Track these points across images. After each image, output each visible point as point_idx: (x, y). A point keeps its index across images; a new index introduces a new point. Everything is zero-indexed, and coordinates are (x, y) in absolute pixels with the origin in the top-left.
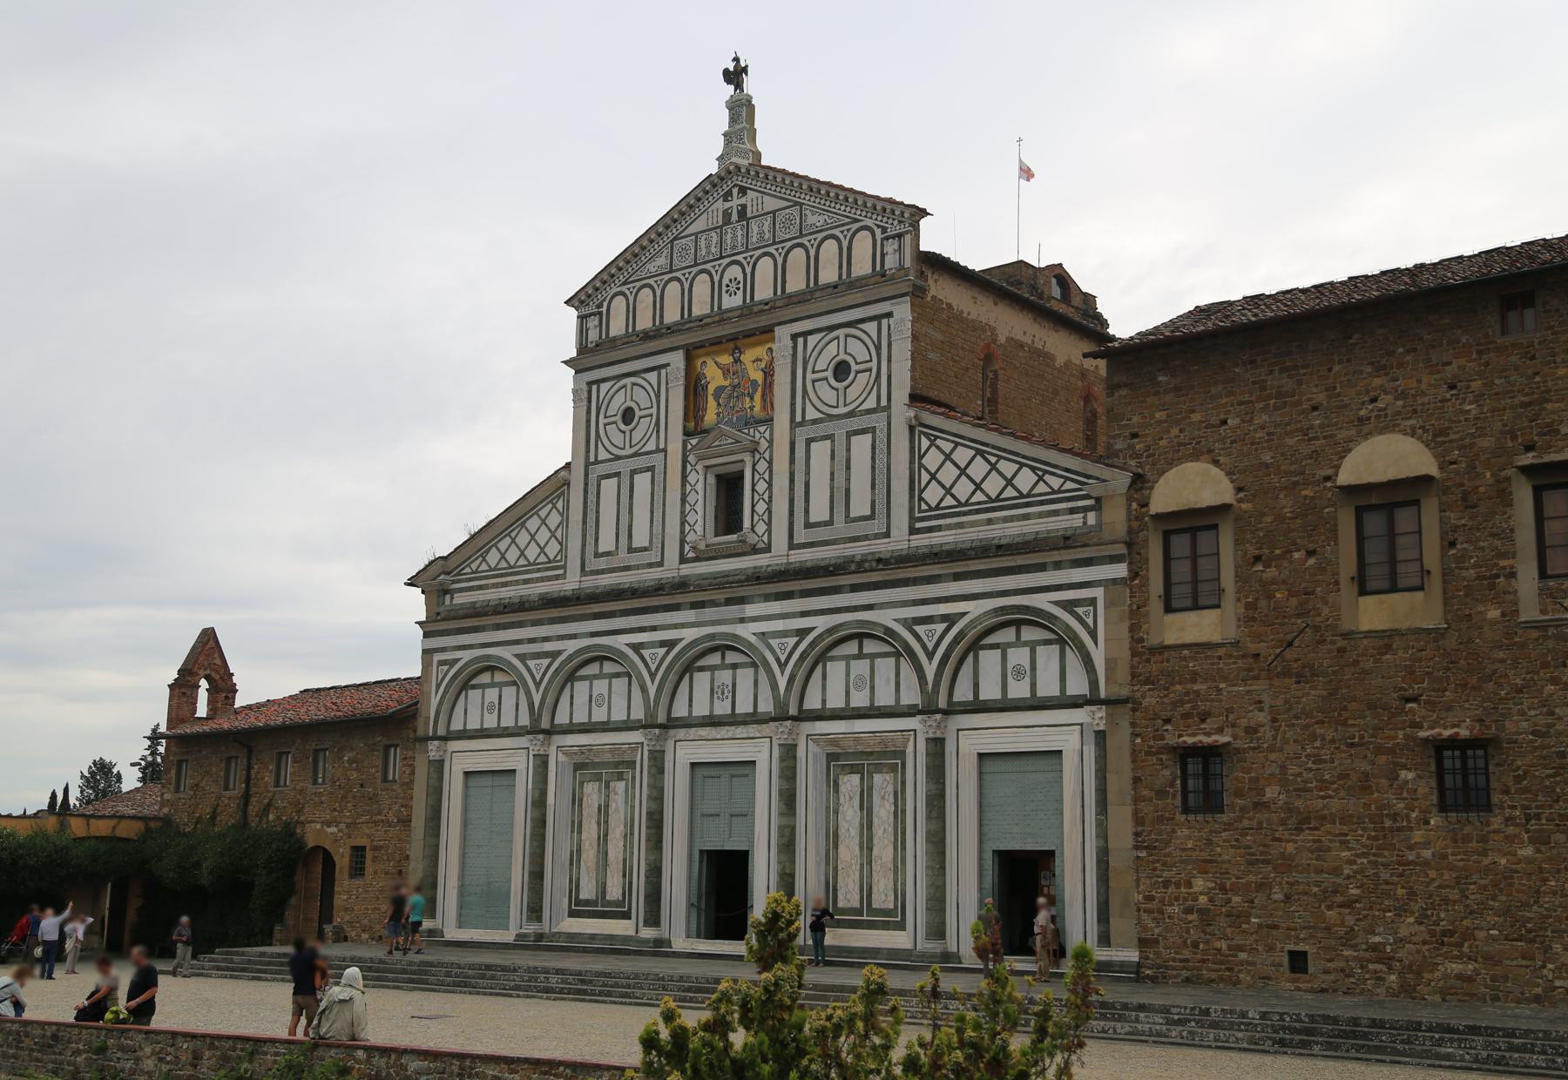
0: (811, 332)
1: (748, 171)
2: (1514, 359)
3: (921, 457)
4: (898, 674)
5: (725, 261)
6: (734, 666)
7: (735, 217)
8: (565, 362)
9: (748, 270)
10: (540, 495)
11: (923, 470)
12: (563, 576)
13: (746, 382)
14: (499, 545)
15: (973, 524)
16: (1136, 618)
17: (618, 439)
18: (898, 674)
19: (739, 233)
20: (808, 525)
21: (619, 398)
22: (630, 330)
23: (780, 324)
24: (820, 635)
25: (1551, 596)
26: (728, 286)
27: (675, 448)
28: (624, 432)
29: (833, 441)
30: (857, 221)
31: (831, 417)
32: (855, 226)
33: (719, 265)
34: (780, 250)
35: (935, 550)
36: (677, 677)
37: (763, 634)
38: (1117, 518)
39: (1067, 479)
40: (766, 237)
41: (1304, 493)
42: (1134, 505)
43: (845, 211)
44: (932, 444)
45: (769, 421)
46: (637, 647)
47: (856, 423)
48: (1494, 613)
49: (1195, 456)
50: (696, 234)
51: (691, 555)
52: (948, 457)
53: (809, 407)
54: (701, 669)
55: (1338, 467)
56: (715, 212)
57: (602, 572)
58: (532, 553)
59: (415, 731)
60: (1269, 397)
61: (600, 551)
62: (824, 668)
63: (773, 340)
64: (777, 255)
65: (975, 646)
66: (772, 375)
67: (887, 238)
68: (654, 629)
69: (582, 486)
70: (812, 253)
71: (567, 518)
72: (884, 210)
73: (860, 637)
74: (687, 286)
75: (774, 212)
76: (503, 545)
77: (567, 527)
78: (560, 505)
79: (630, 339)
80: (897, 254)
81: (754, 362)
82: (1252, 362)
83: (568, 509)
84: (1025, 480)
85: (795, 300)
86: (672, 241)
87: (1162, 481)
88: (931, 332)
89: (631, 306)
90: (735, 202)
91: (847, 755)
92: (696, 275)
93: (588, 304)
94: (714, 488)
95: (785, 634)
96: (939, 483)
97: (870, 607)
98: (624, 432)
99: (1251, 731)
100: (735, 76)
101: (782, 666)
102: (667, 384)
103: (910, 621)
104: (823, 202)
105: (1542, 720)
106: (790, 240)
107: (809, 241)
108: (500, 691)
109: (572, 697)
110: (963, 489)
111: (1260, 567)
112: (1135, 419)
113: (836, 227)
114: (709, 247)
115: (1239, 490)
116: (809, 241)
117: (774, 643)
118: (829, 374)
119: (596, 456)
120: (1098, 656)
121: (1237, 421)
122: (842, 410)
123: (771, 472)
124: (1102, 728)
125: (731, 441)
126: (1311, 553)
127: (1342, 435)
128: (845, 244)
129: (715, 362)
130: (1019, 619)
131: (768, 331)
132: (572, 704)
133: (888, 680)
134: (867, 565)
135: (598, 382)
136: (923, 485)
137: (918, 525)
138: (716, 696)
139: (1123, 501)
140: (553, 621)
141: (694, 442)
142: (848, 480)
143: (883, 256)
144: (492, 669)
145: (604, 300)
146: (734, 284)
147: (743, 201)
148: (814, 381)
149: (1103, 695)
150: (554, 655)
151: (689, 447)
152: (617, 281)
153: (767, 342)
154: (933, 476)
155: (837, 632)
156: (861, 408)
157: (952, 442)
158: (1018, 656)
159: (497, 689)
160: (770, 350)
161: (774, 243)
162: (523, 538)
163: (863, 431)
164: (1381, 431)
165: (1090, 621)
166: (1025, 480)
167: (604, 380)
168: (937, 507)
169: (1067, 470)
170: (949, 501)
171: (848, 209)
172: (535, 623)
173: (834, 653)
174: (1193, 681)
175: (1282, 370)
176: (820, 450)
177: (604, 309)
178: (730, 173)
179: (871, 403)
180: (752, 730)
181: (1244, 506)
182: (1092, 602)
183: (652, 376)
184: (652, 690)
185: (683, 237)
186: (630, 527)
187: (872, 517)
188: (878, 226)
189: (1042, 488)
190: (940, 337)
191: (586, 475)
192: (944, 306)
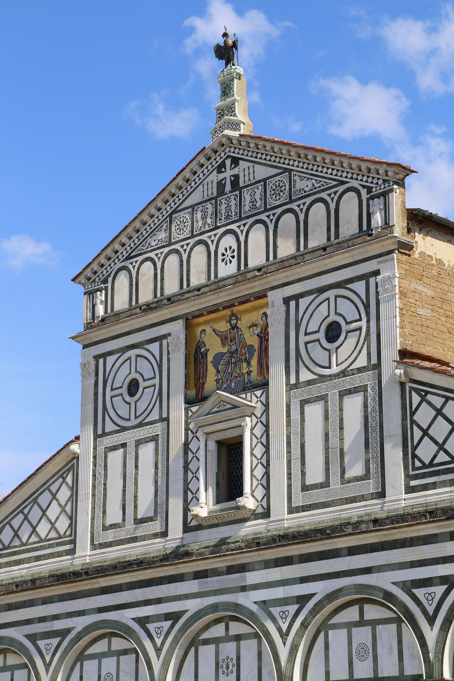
1: (240, 142)
3: (413, 413)
4: (400, 642)
5: (220, 231)
6: (238, 638)
7: (228, 188)
8: (73, 338)
9: (242, 238)
10: (52, 469)
11: (415, 427)
12: (72, 552)
13: (243, 347)
14: (12, 523)
17: (123, 410)
18: (400, 642)
19: (233, 203)
20: (305, 488)
21: (125, 370)
22: (134, 303)
23: (272, 288)
24: (320, 602)
26: (223, 255)
28: (129, 404)
29: (326, 402)
30: (343, 183)
31: (323, 378)
32: (341, 189)
33: (215, 235)
34: (271, 217)
35: (430, 508)
36: (182, 652)
37: (264, 602)
40: (258, 205)
43: (331, 174)
44: (423, 399)
50: (193, 207)
51: (194, 523)
52: (439, 412)
54: (206, 642)
56: (210, 184)
61: (108, 523)
62: (326, 636)
63: (266, 305)
64: (268, 222)
66: (267, 340)
67: (372, 198)
68: (159, 601)
70: (302, 217)
71: (77, 492)
72: (369, 171)
73: (361, 602)
75: (264, 180)
76: (16, 523)
77: (77, 501)
78: (69, 479)
79: (134, 311)
81: (250, 328)
83: (77, 483)
85: (286, 264)
88: (420, 288)
90: (228, 173)
92: (194, 246)
93: (94, 281)
94: (215, 455)
95: (285, 601)
96: (432, 439)
97: (367, 571)
98: (129, 404)
101: (284, 635)
102: (168, 354)
103: (409, 585)
104: (310, 167)
107: (299, 206)
108: (12, 675)
109: (81, 677)
113: (324, 190)
116: (299, 206)
117: (275, 611)
118: (321, 335)
119: (104, 428)
122: (335, 369)
123: (268, 436)
125: (228, 406)
128: (333, 206)
129: (213, 330)
131: (262, 295)
133: (391, 648)
134: (363, 527)
135: (105, 355)
136: (416, 441)
137: (413, 483)
138: (221, 671)
140: (63, 598)
141: (194, 409)
142: (342, 439)
143: (369, 216)
145: (109, 275)
146: (229, 253)
147: (235, 171)
148: (306, 343)
150: (63, 633)
151: (190, 414)
152: (120, 257)
153: (261, 307)
154: (425, 433)
155: (336, 598)
156: (351, 368)
157: (443, 396)
160: (265, 314)
161: (266, 210)
162: (35, 515)
167: (110, 353)
168: (431, 464)
170: (442, 457)
171: (335, 172)
172: (46, 601)
173: (335, 620)
178: (223, 145)
179: (362, 362)
183: (154, 347)
184: (157, 665)
186: (136, 497)
187: (366, 476)
188: (364, 187)
190: (430, 293)
191: (95, 448)
192: (434, 262)
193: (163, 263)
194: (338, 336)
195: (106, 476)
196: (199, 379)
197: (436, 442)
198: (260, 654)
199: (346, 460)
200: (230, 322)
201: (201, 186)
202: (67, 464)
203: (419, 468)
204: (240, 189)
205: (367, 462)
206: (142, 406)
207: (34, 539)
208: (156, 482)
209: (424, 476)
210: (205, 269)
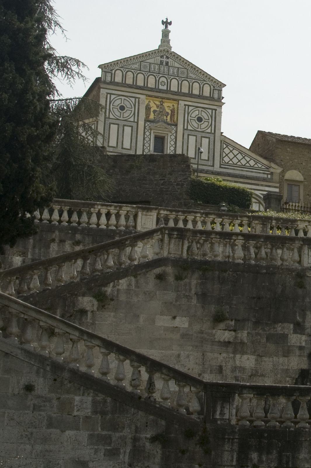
0: (191, 106)
3: (223, 149)
7: (164, 64)
9: (169, 81)
11: (224, 153)
15: (237, 170)
17: (118, 114)
19: (166, 69)
23: (181, 100)
26: (161, 82)
27: (141, 123)
28: (121, 113)
29: (196, 138)
32: (205, 82)
38: (276, 178)
39: (263, 166)
40: (175, 74)
42: (281, 176)
44: (227, 147)
45: (176, 125)
47: (204, 135)
49: (295, 169)
50: (150, 63)
53: (189, 126)
61: (110, 145)
67: (215, 89)
75: (178, 68)
80: (217, 95)
81: (168, 107)
82: (308, 152)
84: (252, 163)
86: (141, 62)
87: (288, 172)
89: (124, 76)
100: (166, 23)
106: (184, 78)
110: (235, 161)
111: (308, 196)
112: (282, 157)
114: (154, 69)
115: (305, 179)
121: (305, 164)
122: (199, 130)
125: (163, 127)
134: (208, 172)
135: (111, 94)
137: (222, 166)
145: (114, 69)
147: (168, 60)
152: (118, 66)
161: (178, 76)
166: (252, 163)
168: (228, 163)
169: (263, 163)
176: (192, 139)
177: (113, 72)
179: (209, 131)
181: (306, 183)
185: (144, 62)
188: (212, 85)
189: (256, 166)
191: (105, 121)
193: (137, 75)
200: (160, 102)
201: (153, 59)
203: (224, 163)
206: (126, 115)
209: (225, 165)
210: (154, 84)
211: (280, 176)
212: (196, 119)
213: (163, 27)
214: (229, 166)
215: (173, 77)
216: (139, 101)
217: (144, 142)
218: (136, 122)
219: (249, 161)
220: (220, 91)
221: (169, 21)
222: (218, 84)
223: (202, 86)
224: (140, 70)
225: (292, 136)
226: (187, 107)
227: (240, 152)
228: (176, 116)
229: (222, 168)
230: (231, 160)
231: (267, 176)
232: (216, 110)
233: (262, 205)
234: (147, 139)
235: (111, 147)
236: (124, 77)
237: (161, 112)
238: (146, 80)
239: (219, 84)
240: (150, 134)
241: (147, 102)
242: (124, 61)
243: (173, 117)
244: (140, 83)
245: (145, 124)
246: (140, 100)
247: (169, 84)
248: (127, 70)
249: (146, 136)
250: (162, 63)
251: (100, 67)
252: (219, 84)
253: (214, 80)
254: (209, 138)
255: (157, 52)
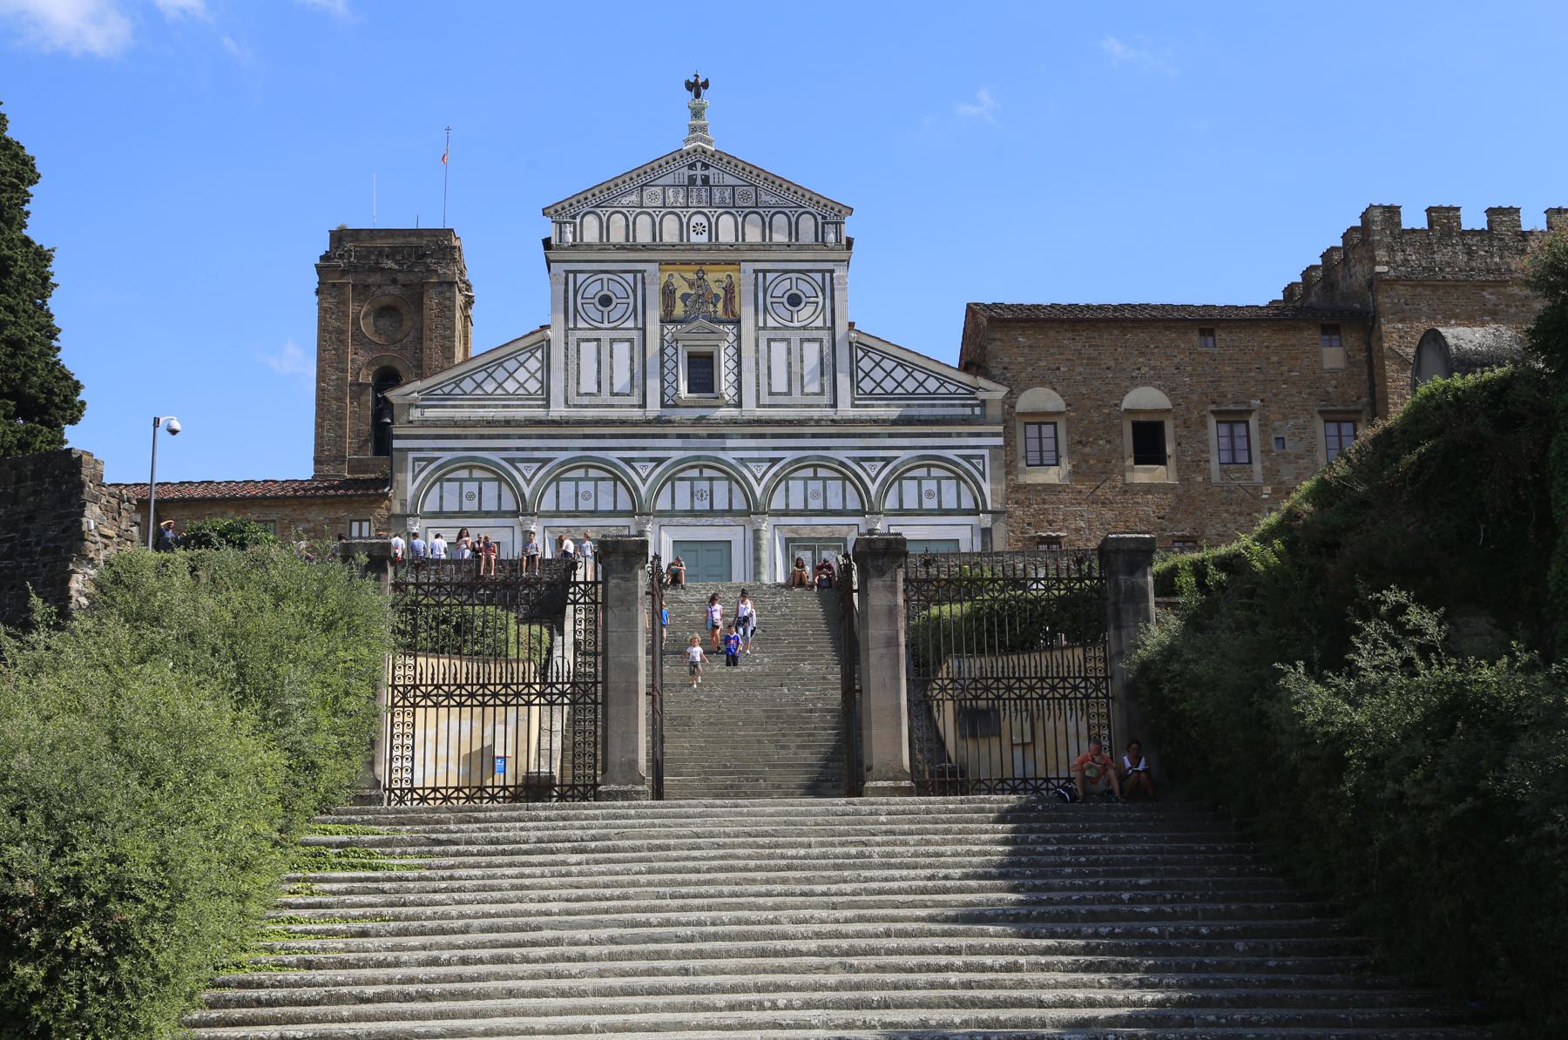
0: (769, 271)
1: (713, 156)
2: (1207, 360)
3: (858, 362)
4: (844, 491)
6: (711, 479)
7: (699, 182)
9: (713, 220)
12: (547, 406)
16: (1010, 468)
17: (597, 316)
18: (844, 491)
19: (704, 194)
20: (771, 394)
22: (605, 240)
23: (744, 261)
25: (1225, 472)
30: (802, 207)
31: (787, 328)
32: (801, 210)
38: (995, 411)
40: (727, 201)
41: (1105, 411)
42: (1006, 407)
45: (737, 322)
46: (628, 461)
47: (807, 334)
48: (1200, 479)
49: (1042, 384)
50: (664, 186)
51: (670, 402)
52: (877, 364)
53: (769, 318)
55: (1122, 400)
57: (586, 406)
58: (510, 386)
59: (388, 509)
60: (1084, 358)
61: (582, 391)
65: (900, 478)
67: (828, 223)
68: (644, 449)
69: (563, 345)
73: (815, 467)
74: (657, 220)
75: (733, 187)
76: (479, 377)
78: (539, 354)
84: (932, 384)
86: (642, 186)
87: (1023, 395)
91: (802, 539)
97: (828, 448)
99: (1077, 530)
100: (696, 87)
105: (1222, 529)
109: (558, 492)
110: (889, 385)
115: (1068, 405)
117: (751, 465)
120: (986, 488)
122: (796, 324)
124: (989, 526)
126: (1108, 442)
127: (1123, 384)
130: (928, 462)
132: (558, 497)
133: (837, 494)
134: (823, 423)
135: (575, 272)
137: (856, 402)
139: (1000, 403)
142: (802, 368)
144: (470, 468)
145: (578, 214)
147: (706, 173)
149: (989, 508)
158: (929, 485)
159: (477, 484)
161: (734, 207)
163: (814, 340)
164: (1144, 385)
165: (981, 468)
166: (932, 384)
167: (581, 272)
168: (871, 393)
173: (795, 475)
174: (1044, 503)
175: (1090, 346)
176: (779, 349)
179: (819, 323)
180: (728, 520)
182: (982, 457)
186: (611, 377)
187: (822, 393)
189: (942, 390)
191: (566, 337)
194: (799, 304)
195: (578, 358)
196: (667, 307)
197: (924, 381)
198: (730, 491)
199: (806, 380)
202: (536, 344)
204: (711, 186)
205: (822, 385)
206: (614, 316)
207: (499, 391)
208: (632, 371)
209: (865, 399)
210: (677, 232)
211: (1003, 406)
212: (785, 300)
213: (690, 95)
214: (876, 399)
215: (721, 211)
216: (643, 278)
217: (662, 373)
218: (639, 329)
219: (924, 381)
220: (838, 224)
221: (700, 81)
222: (832, 209)
223: (793, 220)
224: (641, 207)
225: (1052, 306)
226: (761, 275)
227: (901, 363)
228: (737, 299)
229: (857, 406)
230: (878, 385)
231: (973, 411)
232: (832, 272)
233: (965, 482)
234: (670, 365)
235: (586, 394)
236: (604, 228)
237: (701, 296)
238: (657, 230)
239: (837, 209)
240: (677, 353)
241: (665, 277)
242: (601, 192)
243: (731, 303)
244: (644, 236)
245: (662, 330)
246: (646, 274)
247: (712, 229)
248: (611, 210)
249: (666, 358)
250: (692, 180)
251: (545, 212)
252: (837, 209)
253: (823, 202)
254: (821, 341)
255: (678, 157)
